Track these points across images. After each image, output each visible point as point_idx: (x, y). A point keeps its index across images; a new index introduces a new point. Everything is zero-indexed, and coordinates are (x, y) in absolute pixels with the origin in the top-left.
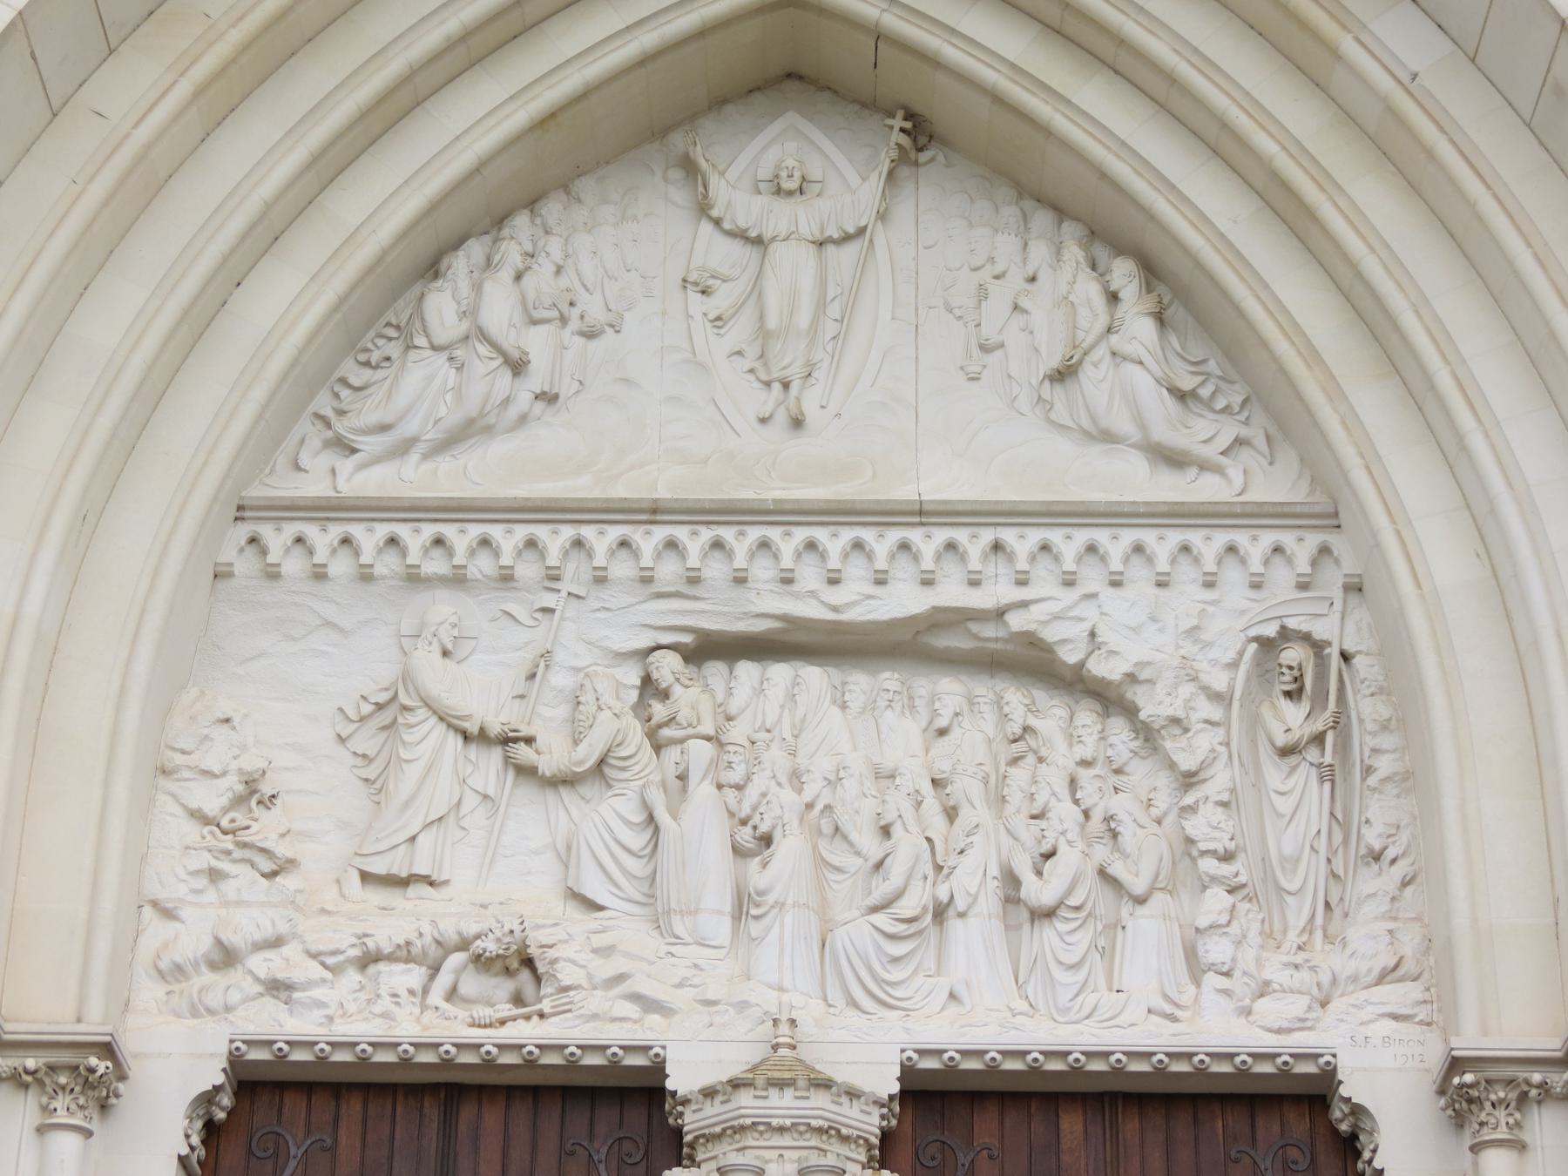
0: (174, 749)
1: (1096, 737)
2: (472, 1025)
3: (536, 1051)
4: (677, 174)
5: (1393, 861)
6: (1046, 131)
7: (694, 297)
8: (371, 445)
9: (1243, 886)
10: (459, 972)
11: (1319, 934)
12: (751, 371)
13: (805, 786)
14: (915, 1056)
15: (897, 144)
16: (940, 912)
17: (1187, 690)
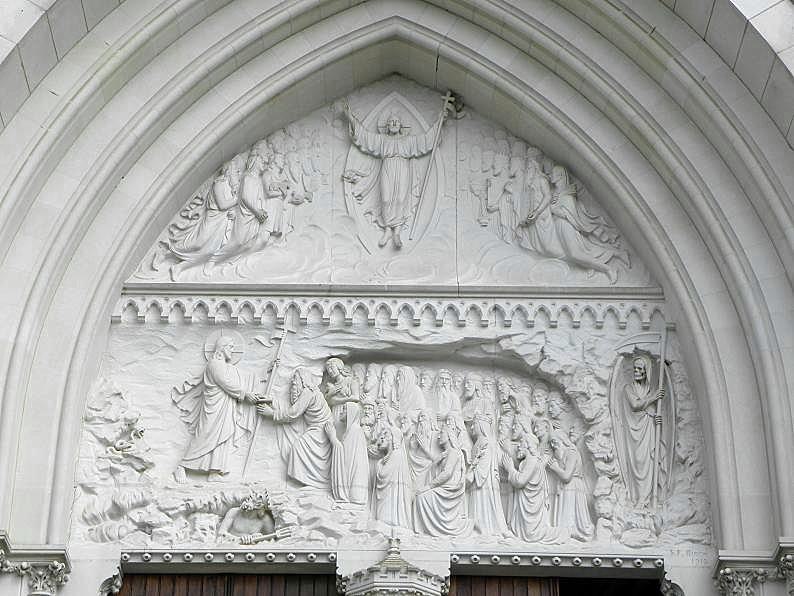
2: (242, 544)
4: (338, 123)
5: (691, 464)
6: (521, 104)
7: (348, 185)
8: (189, 257)
9: (618, 475)
10: (234, 518)
11: (655, 499)
12: (375, 222)
16: (471, 487)
17: (588, 379)
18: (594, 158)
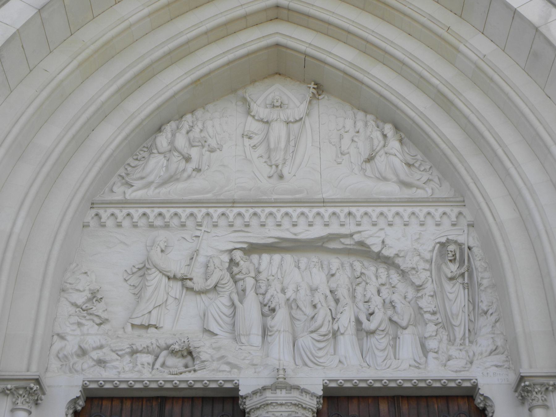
0: (66, 283)
1: (386, 276)
2: (170, 374)
4: (240, 103)
5: (492, 314)
7: (246, 140)
8: (138, 184)
9: (441, 323)
11: (467, 340)
12: (265, 162)
13: (286, 293)
14: (328, 382)
15: (312, 92)
16: (335, 334)
18: (412, 114)
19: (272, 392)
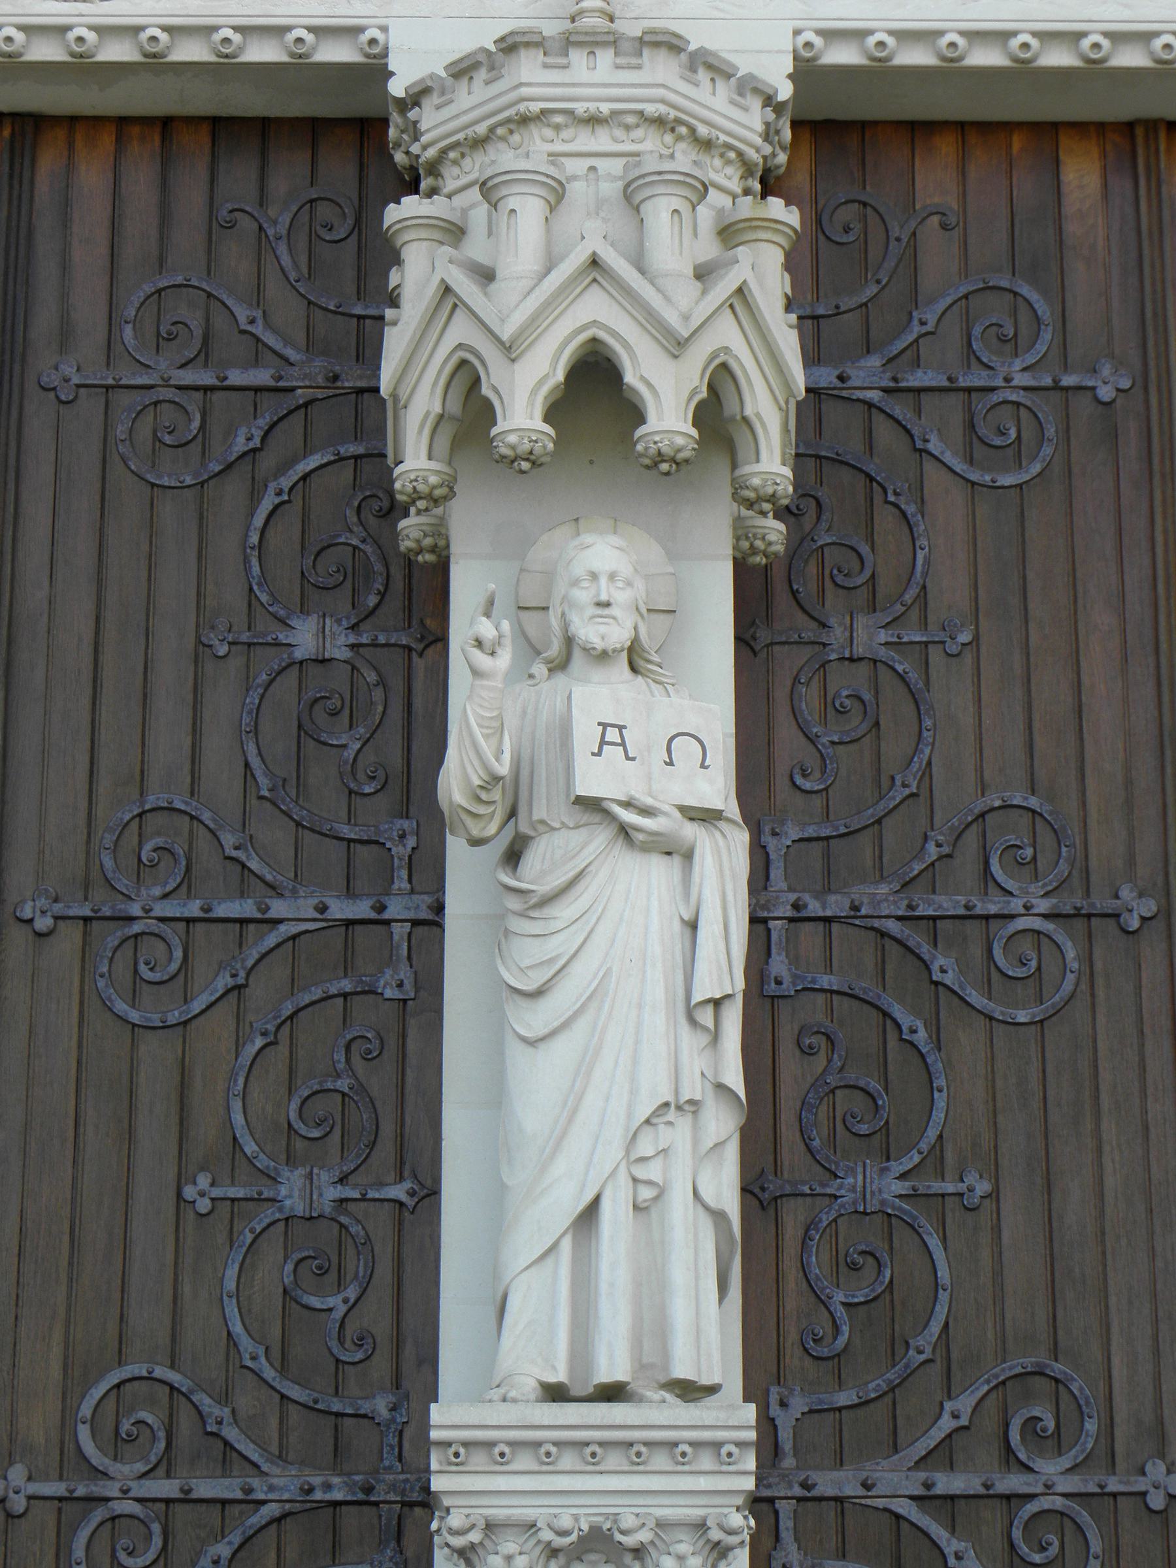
3: (163, 37)
14: (818, 41)
19: (550, 60)
